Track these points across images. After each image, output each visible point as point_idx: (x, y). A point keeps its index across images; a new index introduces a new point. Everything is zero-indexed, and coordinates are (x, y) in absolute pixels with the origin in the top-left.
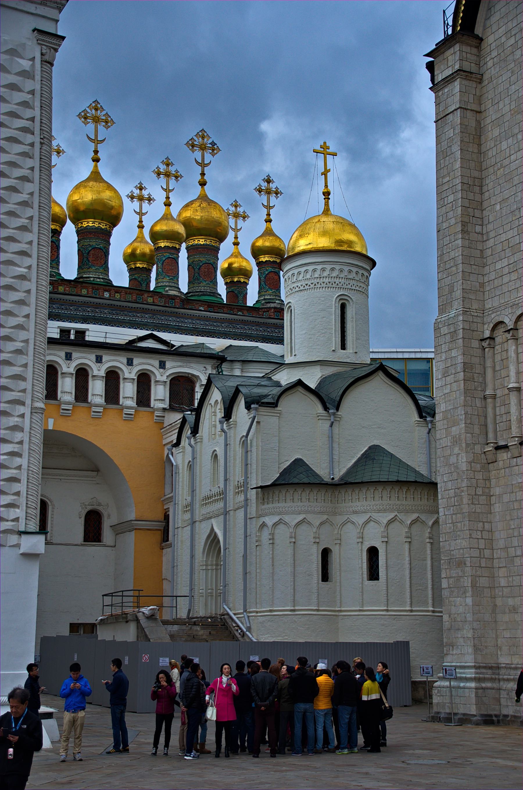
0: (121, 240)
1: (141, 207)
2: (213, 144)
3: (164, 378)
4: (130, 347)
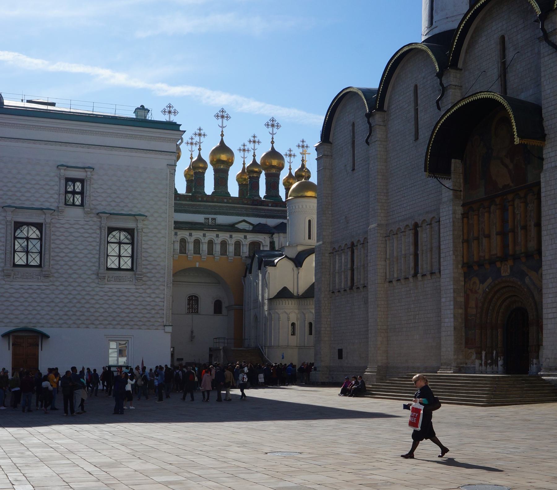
0: (234, 171)
1: (244, 154)
2: (278, 123)
3: (246, 243)
4: (232, 228)
